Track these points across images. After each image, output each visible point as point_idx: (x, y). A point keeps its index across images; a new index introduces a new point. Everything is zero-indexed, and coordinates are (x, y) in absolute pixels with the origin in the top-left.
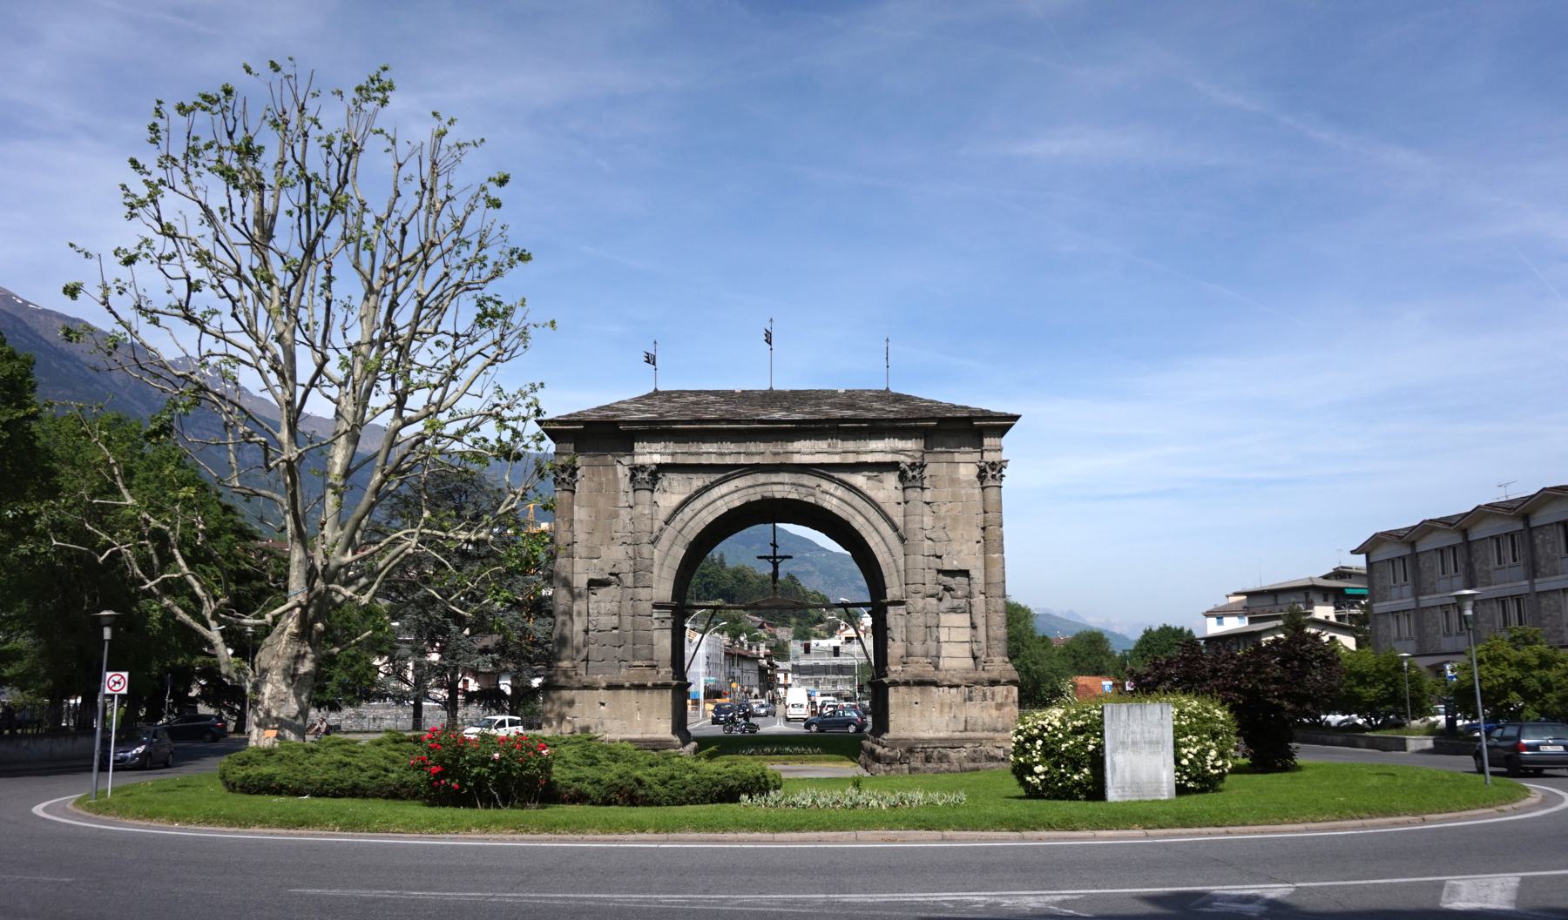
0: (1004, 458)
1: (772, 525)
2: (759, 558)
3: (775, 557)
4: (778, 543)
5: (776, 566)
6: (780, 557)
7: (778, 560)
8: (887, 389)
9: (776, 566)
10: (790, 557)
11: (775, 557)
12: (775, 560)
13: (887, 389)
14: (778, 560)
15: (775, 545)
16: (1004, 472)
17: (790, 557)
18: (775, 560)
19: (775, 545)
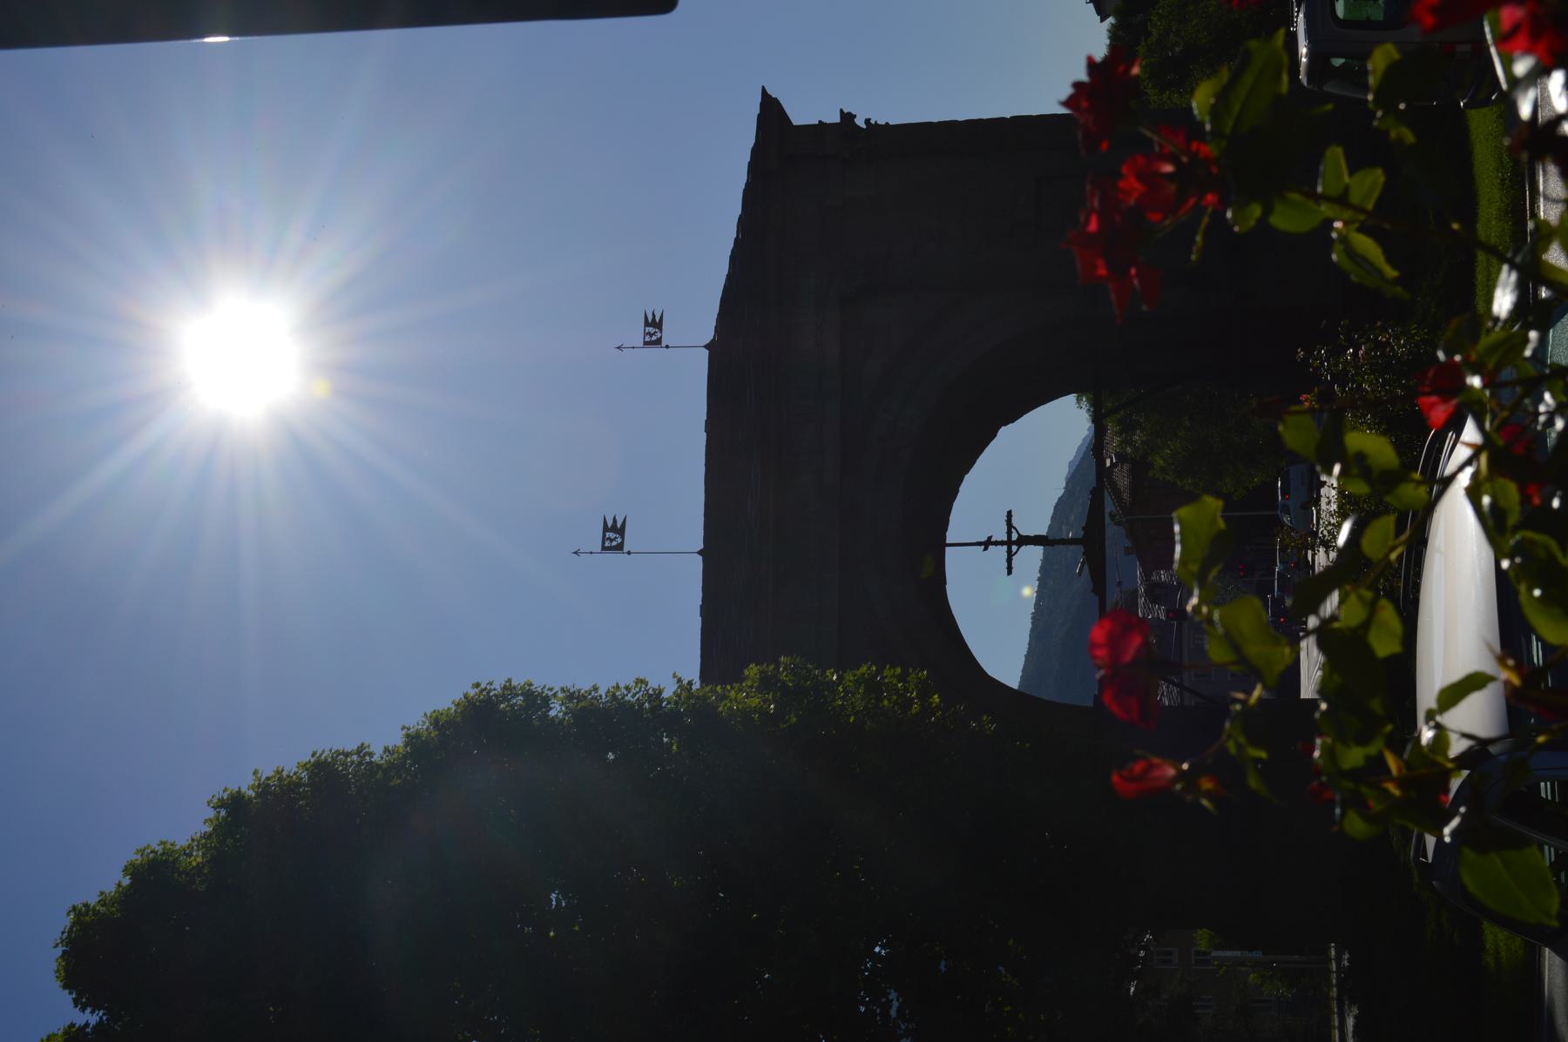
0: (836, 119)
1: (947, 549)
2: (1010, 572)
3: (1009, 543)
4: (984, 539)
5: (1025, 540)
6: (1009, 533)
7: (1015, 537)
8: (706, 347)
9: (1025, 540)
10: (1009, 514)
11: (1009, 543)
12: (1015, 542)
13: (706, 347)
14: (1015, 537)
15: (987, 544)
16: (860, 122)
17: (1009, 514)
18: (1015, 542)
19: (987, 544)
